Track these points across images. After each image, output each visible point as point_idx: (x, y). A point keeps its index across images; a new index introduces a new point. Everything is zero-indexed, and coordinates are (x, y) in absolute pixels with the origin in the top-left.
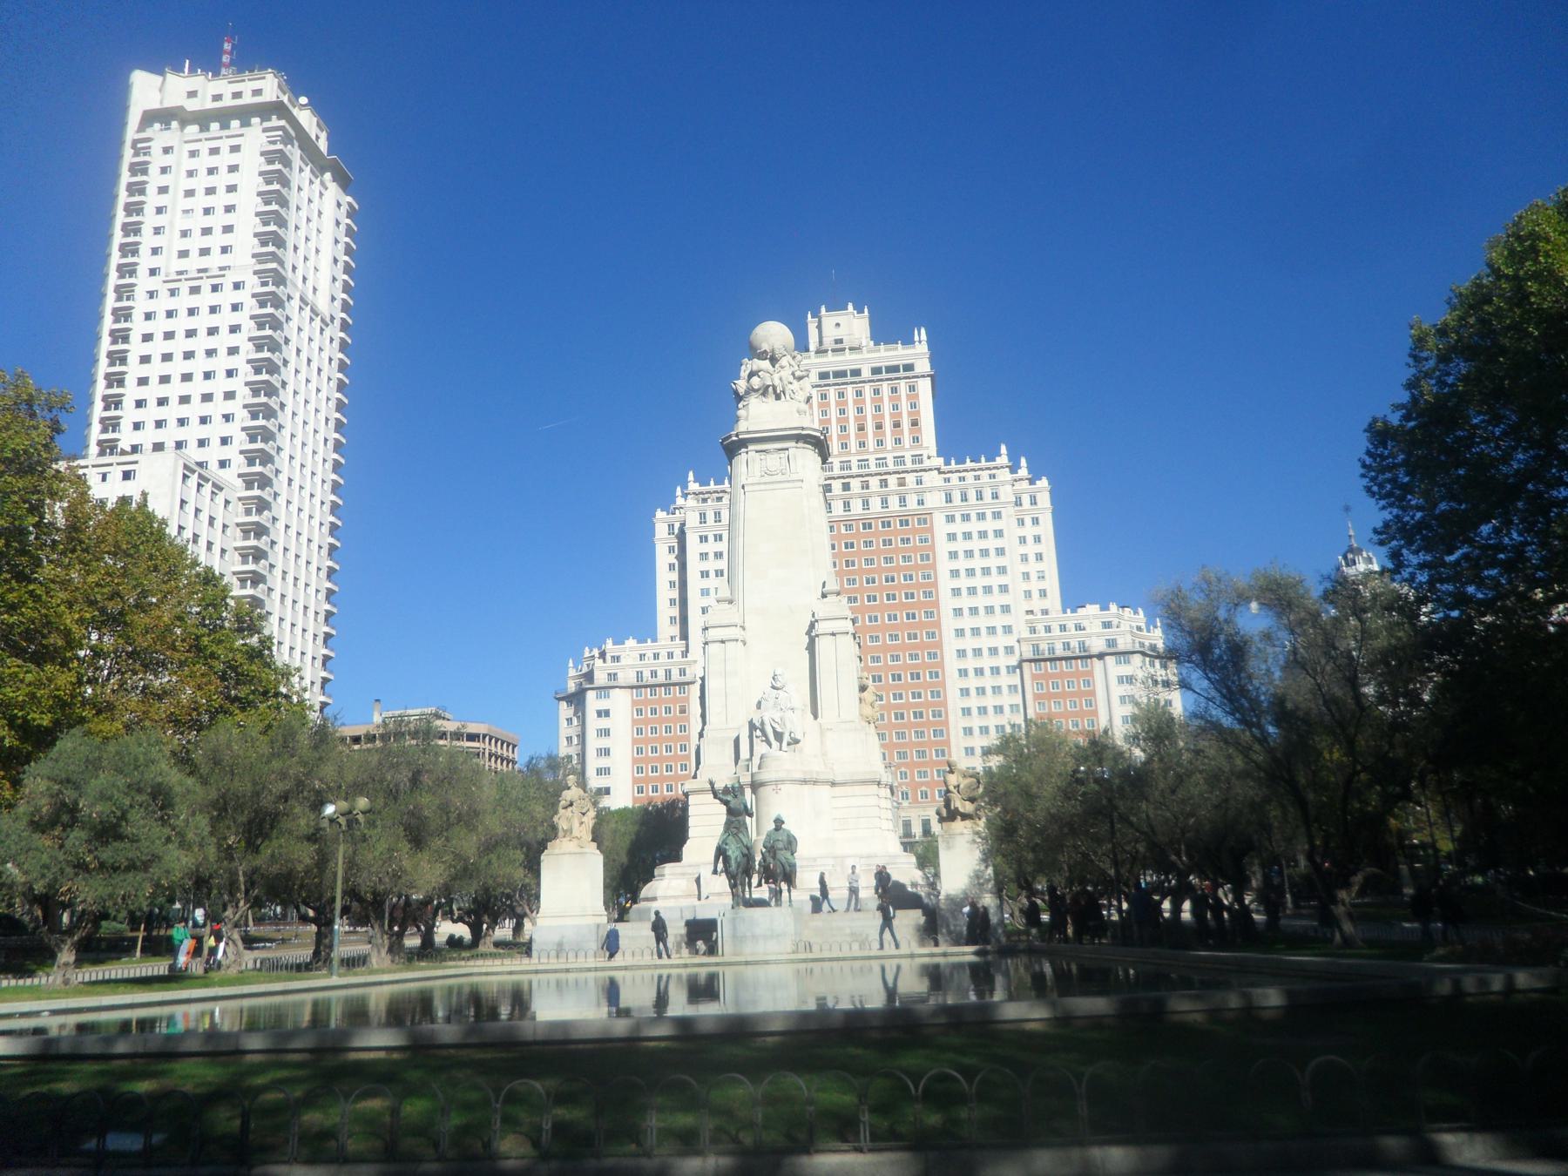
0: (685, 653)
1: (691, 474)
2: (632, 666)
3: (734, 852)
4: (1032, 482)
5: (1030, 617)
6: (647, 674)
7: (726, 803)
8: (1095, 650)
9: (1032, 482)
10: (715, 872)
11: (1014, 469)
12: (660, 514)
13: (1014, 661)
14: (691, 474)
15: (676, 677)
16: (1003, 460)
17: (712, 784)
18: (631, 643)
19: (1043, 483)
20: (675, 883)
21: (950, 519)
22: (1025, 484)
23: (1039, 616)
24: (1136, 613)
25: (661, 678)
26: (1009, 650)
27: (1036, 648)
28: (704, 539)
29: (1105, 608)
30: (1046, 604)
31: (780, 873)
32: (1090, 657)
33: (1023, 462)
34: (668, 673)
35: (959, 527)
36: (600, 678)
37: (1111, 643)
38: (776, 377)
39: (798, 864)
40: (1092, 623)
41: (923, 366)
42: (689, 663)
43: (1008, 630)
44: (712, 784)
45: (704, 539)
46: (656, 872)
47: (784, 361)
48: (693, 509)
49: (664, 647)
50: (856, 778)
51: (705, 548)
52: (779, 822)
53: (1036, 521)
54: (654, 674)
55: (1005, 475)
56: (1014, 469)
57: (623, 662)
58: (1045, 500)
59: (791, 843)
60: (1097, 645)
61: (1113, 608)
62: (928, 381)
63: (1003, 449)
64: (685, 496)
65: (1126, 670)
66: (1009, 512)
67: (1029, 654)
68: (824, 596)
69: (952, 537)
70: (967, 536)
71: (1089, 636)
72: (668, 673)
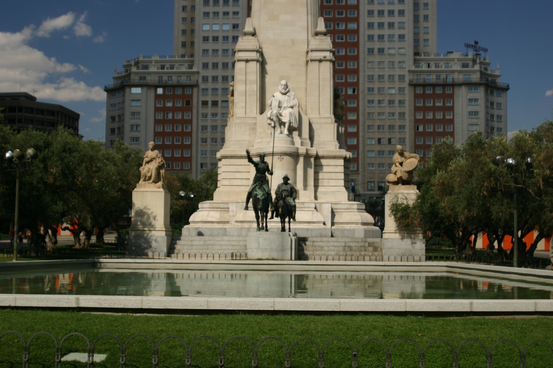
0: (191, 67)
2: (155, 73)
3: (260, 194)
5: (418, 57)
7: (256, 165)
10: (247, 208)
13: (406, 85)
15: (184, 80)
17: (248, 152)
20: (212, 213)
26: (402, 77)
31: (287, 212)
36: (135, 79)
39: (297, 205)
42: (194, 73)
44: (248, 152)
46: (200, 205)
50: (330, 154)
57: (153, 69)
71: (453, 72)
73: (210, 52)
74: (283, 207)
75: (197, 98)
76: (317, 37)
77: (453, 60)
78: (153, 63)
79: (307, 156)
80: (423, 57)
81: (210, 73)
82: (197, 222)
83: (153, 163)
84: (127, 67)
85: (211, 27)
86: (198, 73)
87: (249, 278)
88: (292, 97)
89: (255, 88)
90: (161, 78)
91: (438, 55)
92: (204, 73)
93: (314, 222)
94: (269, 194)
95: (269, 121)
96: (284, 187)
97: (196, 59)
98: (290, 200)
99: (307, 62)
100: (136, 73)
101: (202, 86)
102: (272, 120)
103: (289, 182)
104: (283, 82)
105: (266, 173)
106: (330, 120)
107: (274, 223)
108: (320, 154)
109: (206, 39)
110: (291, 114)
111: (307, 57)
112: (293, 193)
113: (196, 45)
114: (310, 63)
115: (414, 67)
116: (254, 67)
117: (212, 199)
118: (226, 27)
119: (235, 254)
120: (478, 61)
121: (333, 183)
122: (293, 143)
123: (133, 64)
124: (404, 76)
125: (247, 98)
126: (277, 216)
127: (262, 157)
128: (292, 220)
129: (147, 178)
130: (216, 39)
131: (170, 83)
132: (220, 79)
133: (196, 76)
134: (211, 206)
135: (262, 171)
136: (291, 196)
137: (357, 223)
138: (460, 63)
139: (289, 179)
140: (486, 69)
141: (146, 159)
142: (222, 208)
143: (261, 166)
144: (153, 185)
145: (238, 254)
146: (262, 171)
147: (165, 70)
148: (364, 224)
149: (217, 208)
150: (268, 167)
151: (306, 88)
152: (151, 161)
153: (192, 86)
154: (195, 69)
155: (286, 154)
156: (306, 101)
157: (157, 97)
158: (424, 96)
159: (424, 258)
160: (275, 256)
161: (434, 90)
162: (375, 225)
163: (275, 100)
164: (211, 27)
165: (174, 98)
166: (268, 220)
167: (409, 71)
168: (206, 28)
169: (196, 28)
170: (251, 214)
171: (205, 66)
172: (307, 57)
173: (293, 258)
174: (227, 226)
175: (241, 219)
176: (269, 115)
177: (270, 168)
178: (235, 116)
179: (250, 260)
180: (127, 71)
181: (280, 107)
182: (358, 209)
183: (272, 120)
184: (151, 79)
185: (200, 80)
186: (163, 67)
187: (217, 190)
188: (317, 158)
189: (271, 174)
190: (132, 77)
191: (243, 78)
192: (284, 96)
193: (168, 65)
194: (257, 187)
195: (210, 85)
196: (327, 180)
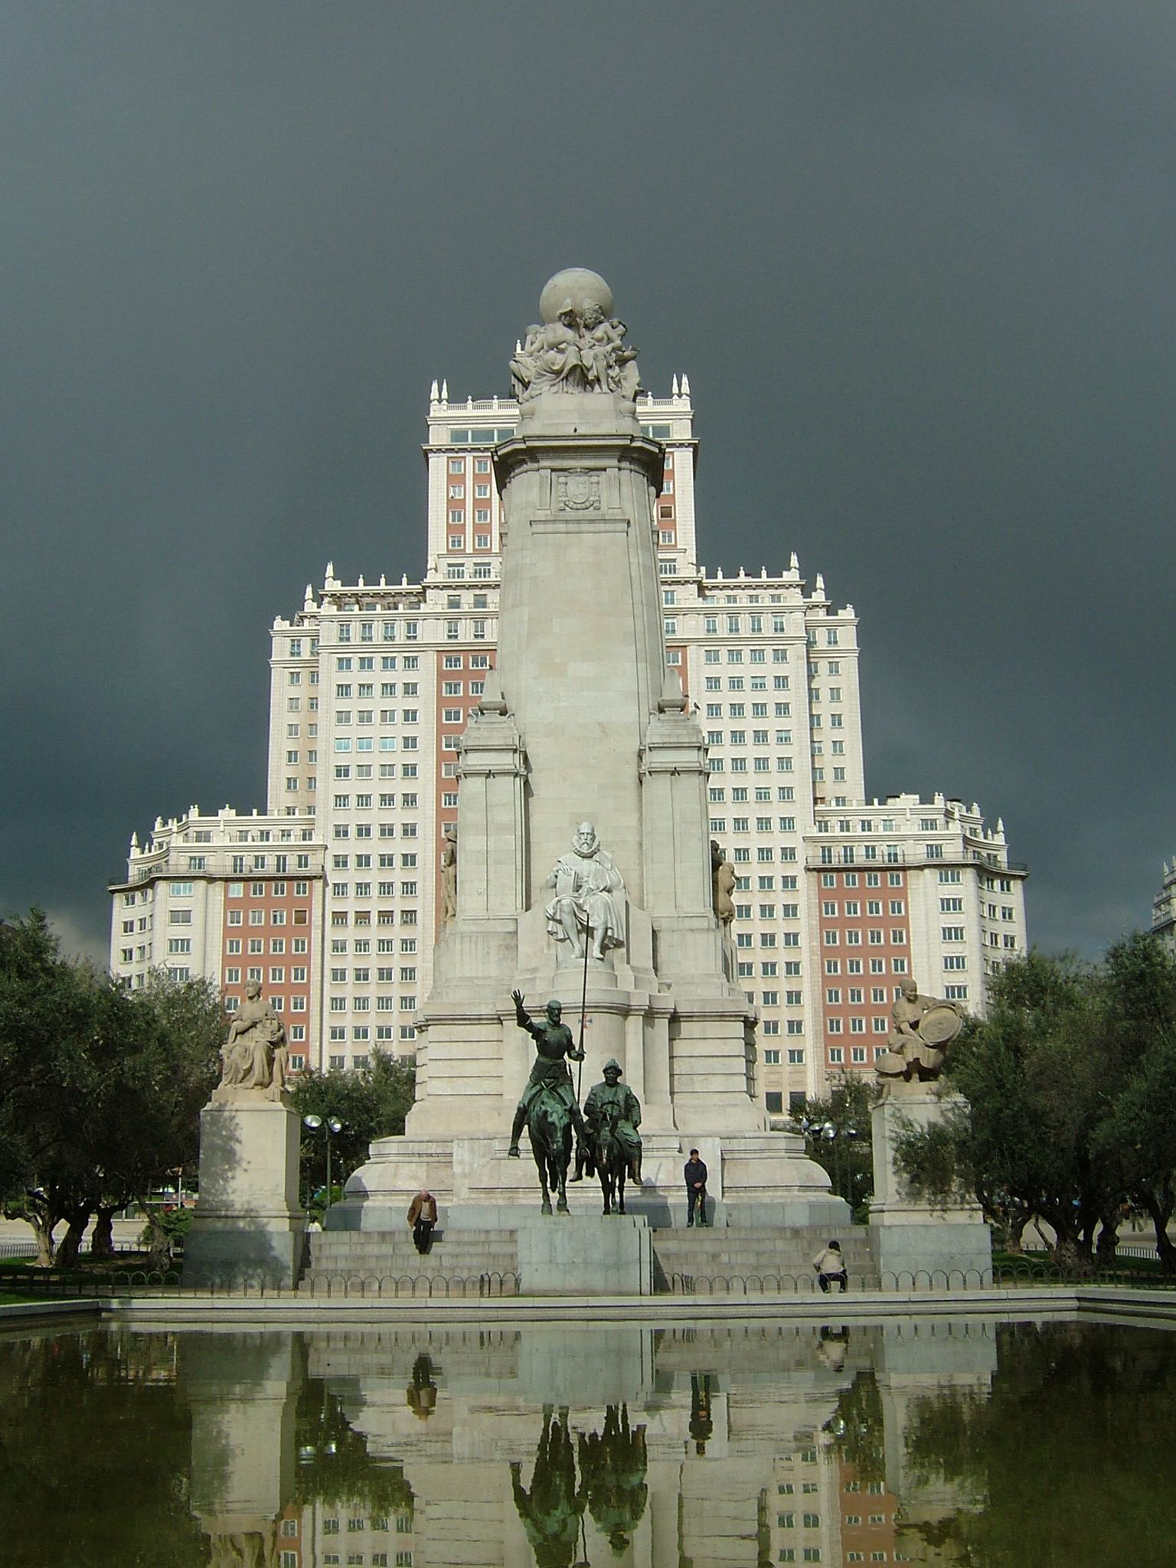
0: (307, 835)
1: (330, 568)
4: (831, 611)
6: (249, 861)
7: (537, 1033)
8: (911, 860)
9: (831, 611)
10: (514, 1151)
11: (807, 590)
12: (280, 624)
13: (797, 870)
14: (330, 568)
15: (292, 867)
16: (792, 576)
17: (518, 999)
18: (227, 814)
19: (848, 614)
20: (406, 1170)
21: (712, 657)
22: (821, 614)
23: (833, 806)
24: (969, 810)
25: (270, 867)
26: (788, 854)
27: (827, 853)
28: (344, 664)
29: (927, 799)
30: (841, 790)
32: (904, 869)
33: (820, 582)
34: (281, 862)
35: (724, 670)
37: (934, 851)
40: (907, 823)
41: (682, 431)
42: (314, 848)
44: (518, 999)
45: (344, 664)
46: (372, 1149)
47: (599, 332)
48: (331, 619)
49: (275, 823)
51: (345, 678)
52: (613, 1073)
53: (834, 669)
54: (260, 861)
55: (795, 597)
56: (807, 590)
58: (848, 638)
60: (915, 853)
61: (939, 801)
62: (688, 454)
63: (794, 561)
64: (319, 599)
65: (950, 891)
66: (796, 653)
67: (818, 863)
68: (661, 710)
70: (736, 683)
71: (903, 838)
72: (281, 862)
74: (610, 1148)
75: (321, 903)
76: (662, 715)
78: (222, 828)
79: (650, 1015)
81: (352, 847)
83: (255, 1033)
87: (525, 1344)
88: (609, 866)
89: (511, 842)
90: (238, 861)
91: (869, 802)
92: (338, 847)
94: (573, 1112)
96: (608, 1095)
97: (319, 816)
98: (625, 1127)
100: (181, 850)
101: (333, 877)
104: (585, 828)
105: (566, 1056)
106: (703, 923)
109: (342, 772)
110: (608, 907)
111: (639, 766)
112: (630, 1109)
114: (647, 779)
115: (816, 829)
116: (509, 788)
117: (401, 1132)
119: (486, 1278)
120: (957, 816)
121: (717, 1084)
122: (614, 979)
123: (175, 829)
125: (491, 869)
126: (590, 1174)
127: (554, 1012)
129: (240, 1076)
130: (364, 770)
131: (259, 872)
133: (320, 854)
135: (555, 1054)
136: (627, 1119)
137: (788, 1187)
138: (917, 819)
139: (619, 1073)
141: (236, 1025)
142: (431, 1155)
143: (551, 1036)
144: (257, 1092)
145: (495, 1278)
147: (249, 843)
150: (569, 1039)
151: (641, 844)
152: (254, 1025)
154: (316, 840)
155: (597, 1008)
156: (641, 876)
157: (229, 902)
159: (988, 1276)
160: (597, 1281)
162: (833, 1191)
166: (567, 1184)
169: (320, 747)
170: (527, 1167)
171: (341, 832)
172: (639, 766)
173: (646, 1288)
177: (576, 1041)
178: (460, 916)
179: (531, 1294)
181: (578, 888)
182: (787, 1150)
183: (560, 922)
185: (330, 865)
187: (415, 1107)
188: (675, 1019)
189: (580, 1057)
190: (173, 854)
191: (480, 818)
192: (586, 861)
194: (544, 1093)
195: (352, 876)
196: (701, 1078)
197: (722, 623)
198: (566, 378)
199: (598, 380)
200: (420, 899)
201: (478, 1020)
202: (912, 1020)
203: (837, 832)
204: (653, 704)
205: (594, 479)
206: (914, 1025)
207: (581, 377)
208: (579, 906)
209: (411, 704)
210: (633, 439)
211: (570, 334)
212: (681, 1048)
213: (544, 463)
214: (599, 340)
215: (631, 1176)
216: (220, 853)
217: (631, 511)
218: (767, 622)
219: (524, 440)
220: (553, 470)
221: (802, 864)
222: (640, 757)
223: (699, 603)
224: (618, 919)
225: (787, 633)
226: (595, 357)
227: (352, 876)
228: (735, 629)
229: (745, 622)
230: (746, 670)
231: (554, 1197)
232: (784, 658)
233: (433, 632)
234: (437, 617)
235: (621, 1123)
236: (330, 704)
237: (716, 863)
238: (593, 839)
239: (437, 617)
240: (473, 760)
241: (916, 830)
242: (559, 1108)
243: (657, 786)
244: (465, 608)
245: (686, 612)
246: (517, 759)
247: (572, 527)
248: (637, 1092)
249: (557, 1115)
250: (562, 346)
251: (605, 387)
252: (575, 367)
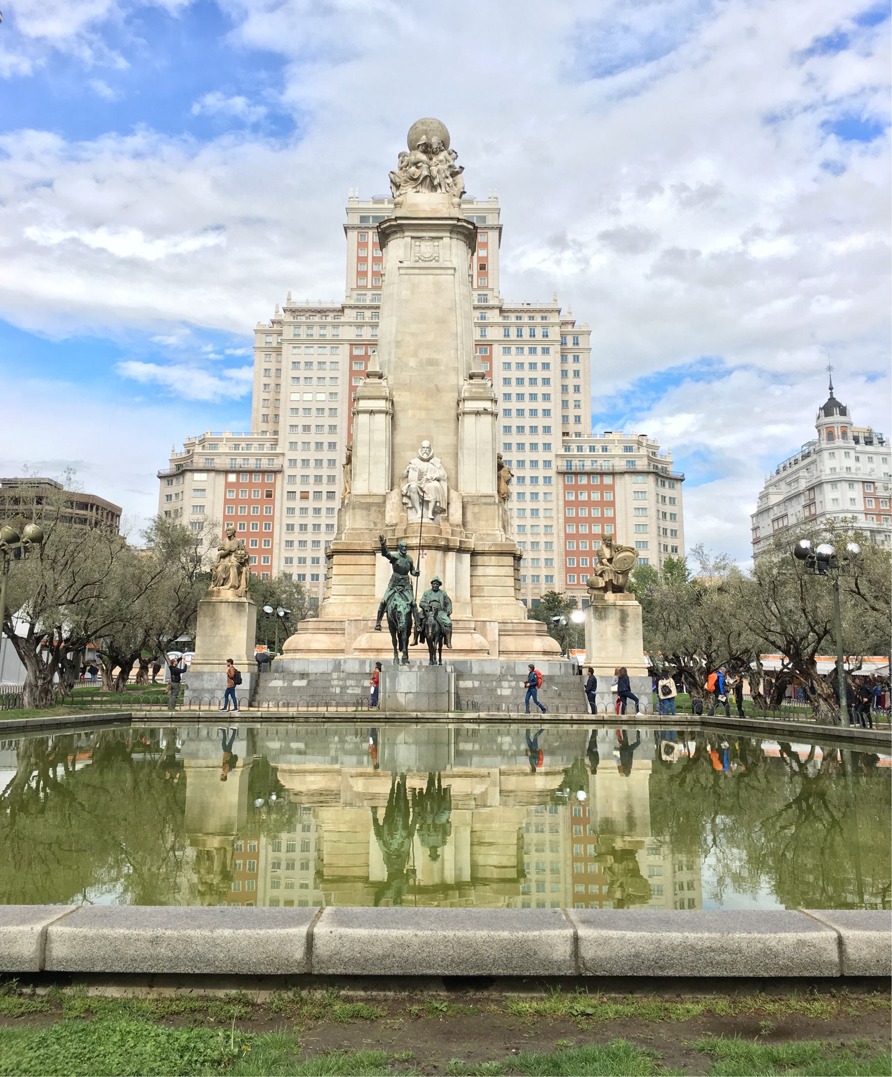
2: (226, 454)
5: (566, 438)
7: (393, 560)
8: (618, 469)
13: (552, 473)
15: (265, 464)
20: (319, 637)
21: (507, 351)
23: (574, 438)
25: (252, 464)
26: (547, 464)
27: (569, 464)
35: (513, 358)
38: (434, 169)
42: (277, 455)
43: (547, 447)
48: (289, 324)
52: (436, 585)
57: (223, 449)
59: (446, 604)
60: (620, 465)
66: (555, 349)
68: (471, 377)
69: (507, 366)
70: (520, 365)
71: (613, 457)
73: (300, 429)
74: (434, 626)
75: (281, 487)
77: (613, 441)
80: (574, 438)
82: (296, 651)
84: (189, 446)
85: (301, 397)
86: (283, 454)
93: (473, 651)
94: (412, 606)
95: (405, 500)
96: (434, 596)
97: (281, 437)
98: (442, 615)
99: (458, 415)
100: (200, 454)
101: (288, 472)
102: (409, 498)
103: (440, 588)
107: (419, 652)
108: (479, 549)
113: (281, 419)
115: (563, 450)
116: (381, 421)
118: (321, 397)
120: (644, 444)
123: (197, 442)
124: (550, 462)
126: (422, 641)
128: (444, 647)
131: (246, 467)
132: (312, 463)
133: (281, 458)
134: (316, 625)
135: (403, 572)
136: (445, 610)
138: (621, 446)
139: (440, 584)
140: (654, 454)
146: (403, 572)
147: (240, 451)
148: (545, 653)
149: (326, 629)
151: (457, 454)
153: (275, 472)
154: (279, 451)
156: (457, 472)
157: (228, 485)
158: (577, 488)
161: (589, 480)
163: (413, 469)
164: (301, 397)
165: (250, 485)
166: (409, 647)
167: (557, 456)
168: (296, 397)
169: (282, 397)
170: (385, 638)
174: (340, 657)
175: (364, 645)
176: (405, 491)
180: (188, 451)
183: (409, 498)
184: (221, 463)
185: (286, 464)
186: (236, 447)
188: (474, 554)
189: (417, 574)
192: (426, 463)
193: (243, 444)
195: (299, 471)
197: (513, 332)
198: (421, 183)
199: (440, 185)
200: (337, 485)
201: (362, 552)
202: (608, 556)
203: (575, 452)
204: (466, 375)
205: (436, 243)
206: (610, 560)
207: (430, 183)
208: (421, 489)
209: (334, 374)
210: (459, 220)
211: (424, 157)
212: (480, 571)
213: (407, 234)
214: (441, 161)
215: (446, 643)
216: (223, 457)
217: (455, 262)
218: (539, 332)
219: (396, 219)
220: (412, 238)
221: (554, 469)
222: (458, 405)
223: (500, 320)
224: (443, 496)
225: (550, 338)
226: (438, 172)
227: (299, 471)
228: (520, 335)
229: (526, 332)
230: (527, 358)
231: (401, 655)
232: (548, 352)
233: (349, 333)
234: (350, 324)
235: (440, 613)
236: (288, 372)
237: (500, 467)
238: (430, 451)
239: (350, 324)
240: (363, 404)
241: (621, 452)
242: (404, 603)
243: (469, 420)
244: (367, 320)
245: (492, 325)
246: (389, 405)
247: (422, 271)
248: (450, 595)
249: (402, 607)
250: (419, 165)
251: (443, 189)
252: (426, 177)
